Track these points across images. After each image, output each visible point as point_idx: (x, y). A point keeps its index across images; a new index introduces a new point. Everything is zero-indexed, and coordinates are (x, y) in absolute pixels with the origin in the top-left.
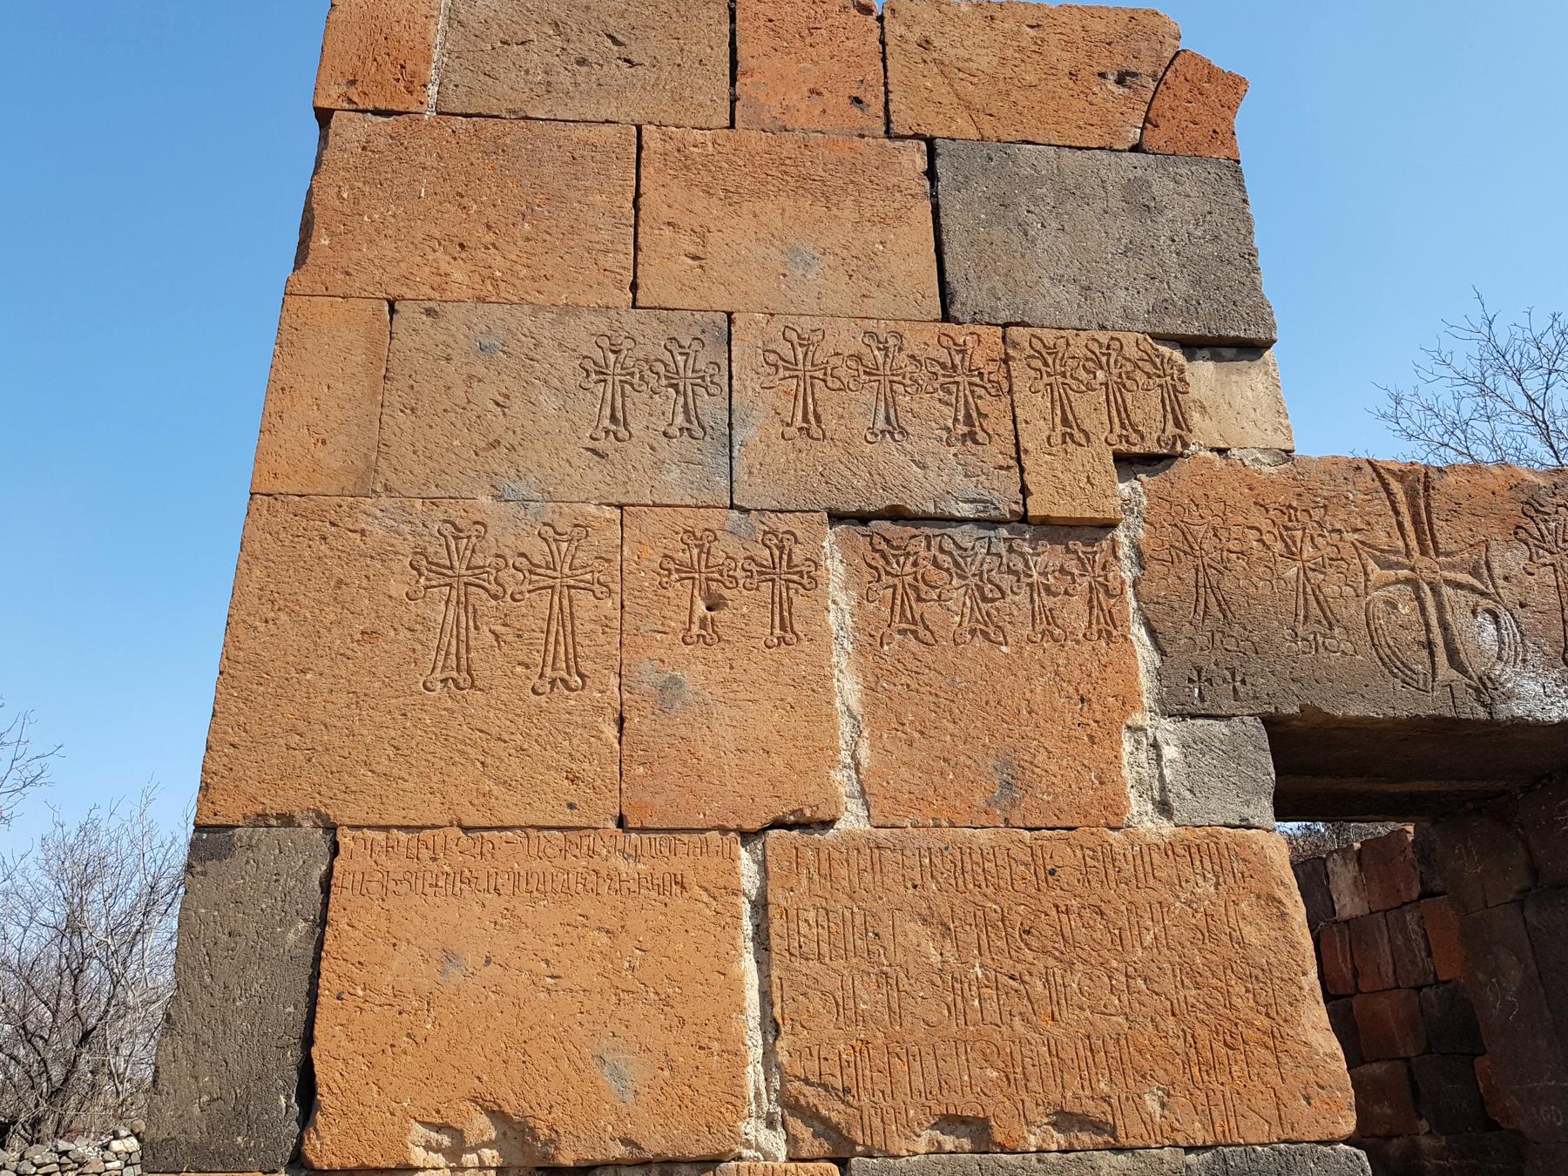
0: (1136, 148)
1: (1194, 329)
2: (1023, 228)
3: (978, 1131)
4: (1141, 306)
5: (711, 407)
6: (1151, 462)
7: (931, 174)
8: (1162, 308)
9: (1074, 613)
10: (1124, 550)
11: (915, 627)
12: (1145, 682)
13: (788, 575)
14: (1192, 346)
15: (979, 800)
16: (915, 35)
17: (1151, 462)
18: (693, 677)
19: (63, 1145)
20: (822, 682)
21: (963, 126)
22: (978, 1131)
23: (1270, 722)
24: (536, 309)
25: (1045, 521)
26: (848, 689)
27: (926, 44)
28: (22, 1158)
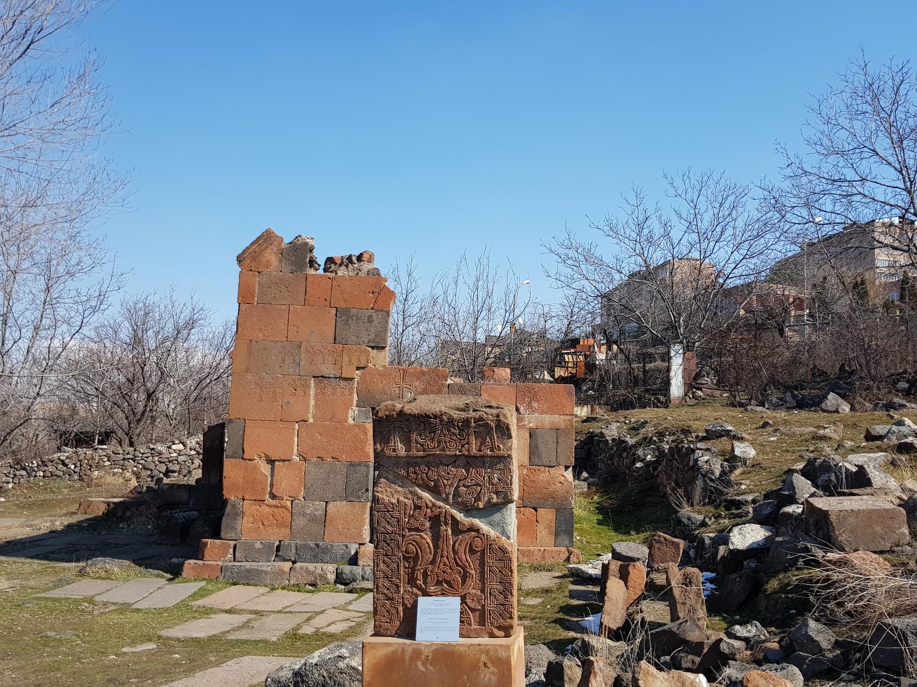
3: (322, 458)
4: (366, 340)
5: (297, 358)
6: (363, 368)
8: (369, 341)
9: (347, 392)
11: (323, 394)
12: (355, 403)
14: (373, 348)
17: (363, 368)
18: (291, 401)
19: (152, 446)
20: (308, 402)
21: (343, 305)
22: (322, 458)
26: (312, 402)
28: (135, 450)
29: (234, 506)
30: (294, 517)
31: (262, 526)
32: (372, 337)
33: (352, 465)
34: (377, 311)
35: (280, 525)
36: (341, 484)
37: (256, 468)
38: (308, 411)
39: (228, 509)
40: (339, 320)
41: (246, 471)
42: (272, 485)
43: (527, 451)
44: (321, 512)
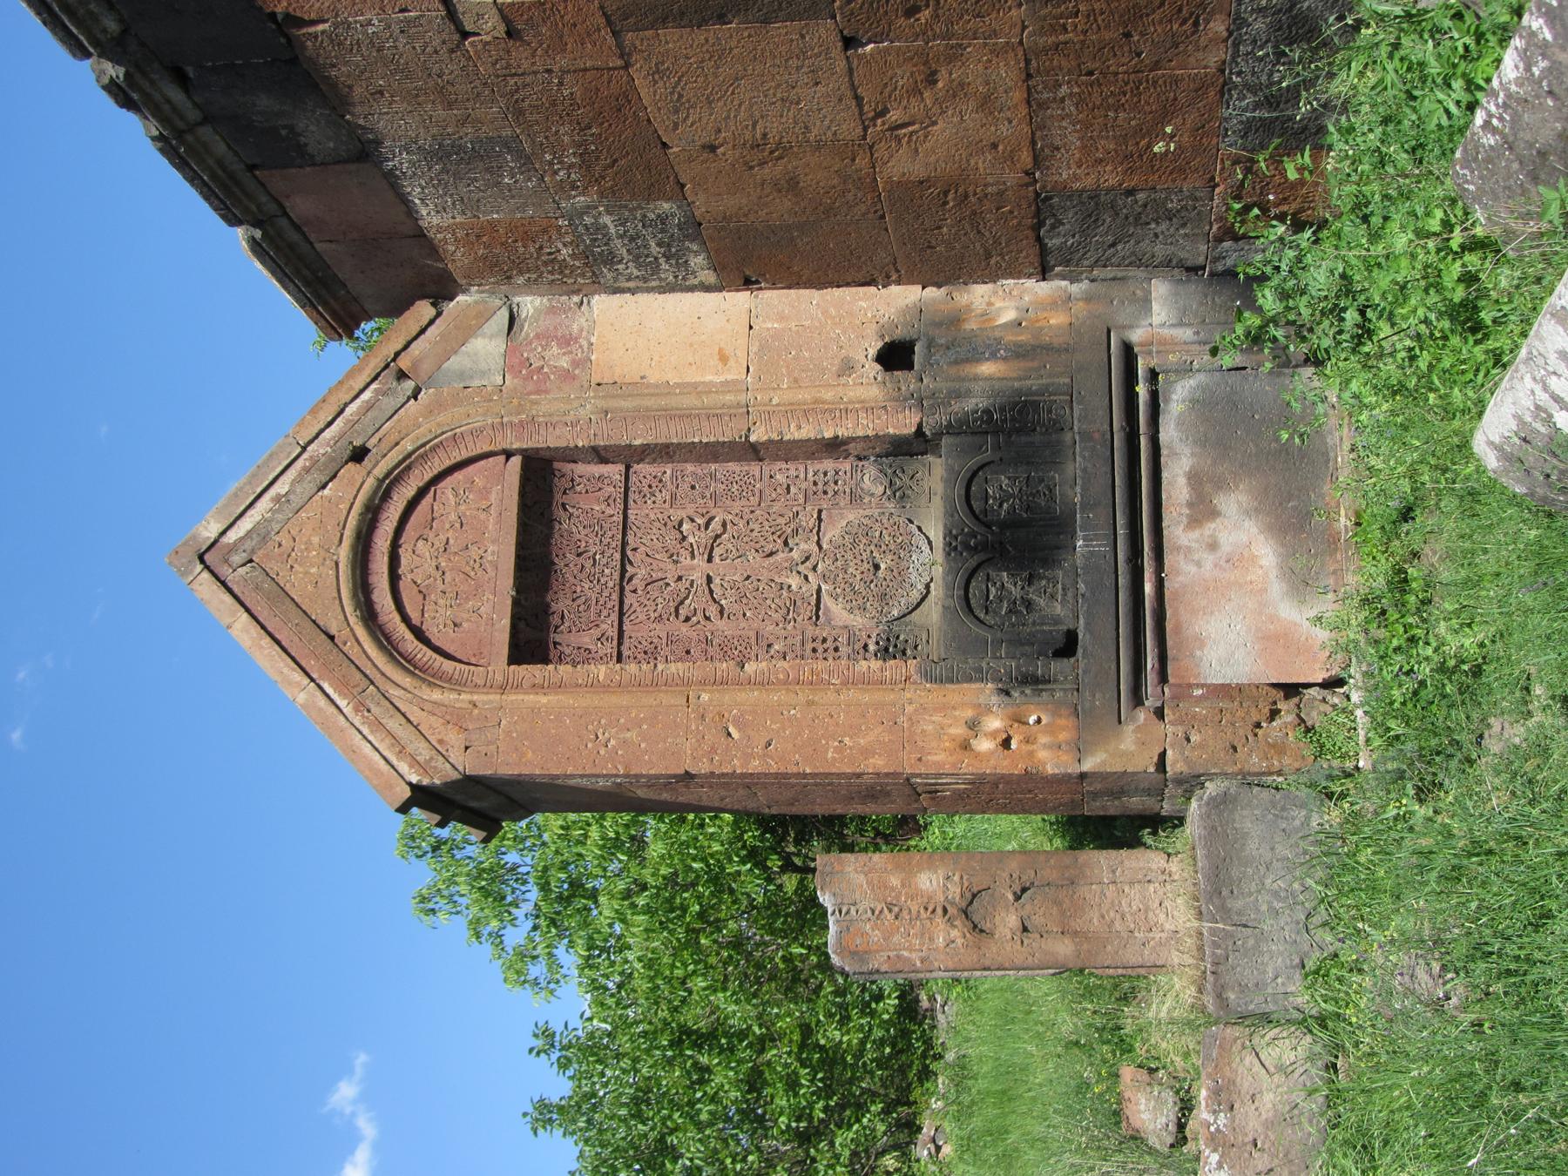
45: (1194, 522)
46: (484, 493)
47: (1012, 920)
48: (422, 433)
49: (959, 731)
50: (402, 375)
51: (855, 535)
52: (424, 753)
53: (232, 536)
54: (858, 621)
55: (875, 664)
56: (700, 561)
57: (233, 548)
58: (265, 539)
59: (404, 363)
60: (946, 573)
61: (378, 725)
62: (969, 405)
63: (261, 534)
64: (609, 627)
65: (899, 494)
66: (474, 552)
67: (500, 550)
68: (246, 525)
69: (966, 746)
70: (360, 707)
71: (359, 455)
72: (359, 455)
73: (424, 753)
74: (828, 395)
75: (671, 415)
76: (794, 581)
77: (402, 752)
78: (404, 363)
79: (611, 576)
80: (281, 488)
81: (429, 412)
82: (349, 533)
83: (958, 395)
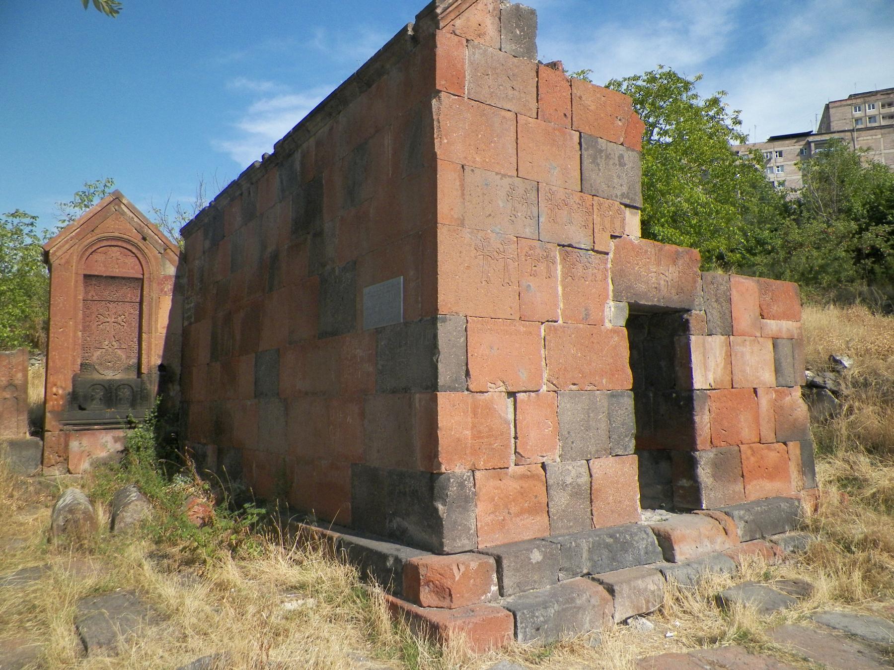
0: (622, 144)
1: (627, 202)
2: (598, 165)
4: (619, 194)
7: (580, 144)
8: (623, 195)
10: (610, 260)
12: (611, 294)
13: (548, 259)
15: (581, 317)
16: (578, 95)
21: (586, 130)
23: (629, 303)
24: (497, 174)
25: (597, 252)
26: (560, 289)
27: (580, 98)
29: (462, 485)
30: (551, 492)
31: (508, 517)
32: (625, 189)
33: (612, 396)
34: (628, 148)
35: (533, 511)
36: (603, 426)
37: (489, 409)
38: (556, 305)
39: (453, 490)
40: (585, 154)
41: (475, 414)
42: (516, 438)
43: (773, 368)
44: (585, 479)
45: (114, 437)
46: (133, 268)
47: (8, 396)
48: (149, 254)
49: (59, 383)
50: (165, 250)
51: (119, 359)
52: (58, 254)
53: (123, 206)
54: (94, 358)
55: (79, 363)
56: (113, 320)
57: (119, 206)
58: (122, 214)
59: (168, 251)
60: (103, 380)
61: (67, 242)
62: (148, 385)
63: (123, 214)
64: (96, 298)
65: (128, 369)
66: (117, 266)
67: (117, 272)
68: (126, 210)
69: (55, 385)
70: (72, 238)
71: (144, 239)
72: (144, 239)
73: (58, 254)
74: (153, 352)
75: (150, 315)
76: (106, 343)
77: (59, 249)
78: (168, 251)
79: (111, 299)
80: (136, 219)
81: (154, 256)
82: (122, 236)
83: (151, 382)
